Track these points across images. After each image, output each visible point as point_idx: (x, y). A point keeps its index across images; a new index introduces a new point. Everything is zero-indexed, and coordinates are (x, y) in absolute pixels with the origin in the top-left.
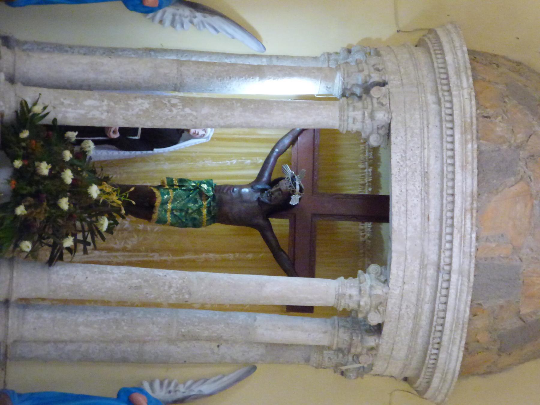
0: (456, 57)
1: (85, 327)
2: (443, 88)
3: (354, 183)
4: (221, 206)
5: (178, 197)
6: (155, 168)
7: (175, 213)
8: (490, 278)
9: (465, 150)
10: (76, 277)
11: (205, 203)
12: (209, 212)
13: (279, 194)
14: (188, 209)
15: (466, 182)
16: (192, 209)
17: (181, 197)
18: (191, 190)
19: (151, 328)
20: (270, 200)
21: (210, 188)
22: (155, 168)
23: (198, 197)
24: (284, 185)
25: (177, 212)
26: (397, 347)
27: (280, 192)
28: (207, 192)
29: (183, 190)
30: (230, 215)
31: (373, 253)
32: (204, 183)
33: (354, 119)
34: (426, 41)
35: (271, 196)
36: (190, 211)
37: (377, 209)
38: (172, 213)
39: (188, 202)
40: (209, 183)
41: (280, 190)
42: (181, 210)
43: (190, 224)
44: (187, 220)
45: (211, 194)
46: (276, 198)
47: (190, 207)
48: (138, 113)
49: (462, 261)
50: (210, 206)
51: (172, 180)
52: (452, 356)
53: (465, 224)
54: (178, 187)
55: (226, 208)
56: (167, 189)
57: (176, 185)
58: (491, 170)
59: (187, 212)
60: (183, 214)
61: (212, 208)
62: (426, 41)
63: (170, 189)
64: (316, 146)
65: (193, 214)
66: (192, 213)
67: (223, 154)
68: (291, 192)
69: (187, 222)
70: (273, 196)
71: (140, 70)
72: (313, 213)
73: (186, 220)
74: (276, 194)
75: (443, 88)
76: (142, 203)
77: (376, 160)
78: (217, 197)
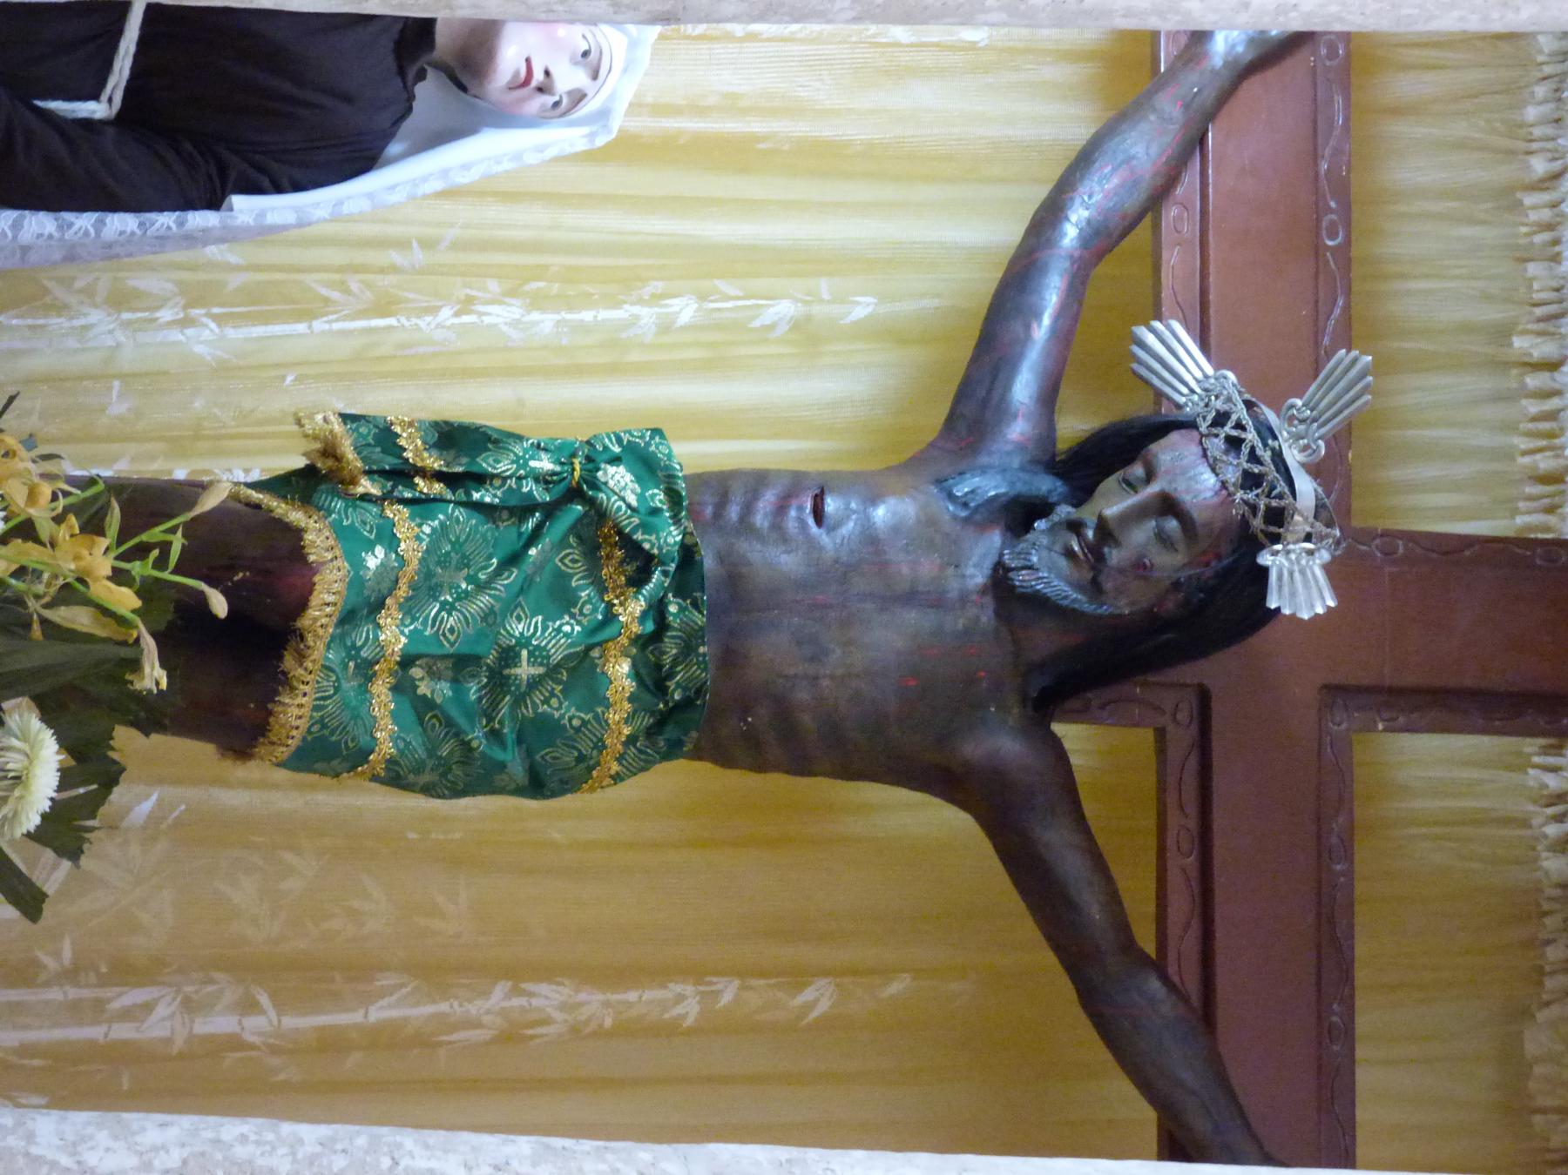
5: (443, 562)
7: (423, 689)
11: (633, 610)
12: (652, 679)
13: (1162, 538)
14: (509, 656)
16: (538, 655)
17: (465, 562)
18: (525, 508)
20: (1094, 588)
21: (658, 497)
23: (572, 562)
24: (1195, 475)
25: (433, 674)
27: (1172, 524)
28: (645, 527)
29: (479, 507)
30: (802, 695)
32: (615, 460)
35: (1096, 555)
36: (525, 670)
38: (402, 687)
39: (511, 606)
40: (647, 465)
41: (1168, 505)
42: (462, 664)
43: (514, 761)
44: (490, 738)
45: (673, 536)
46: (1140, 567)
47: (524, 642)
50: (662, 625)
51: (386, 436)
54: (438, 488)
55: (774, 650)
56: (366, 498)
57: (422, 472)
59: (499, 682)
60: (473, 691)
61: (671, 649)
63: (387, 497)
65: (538, 697)
66: (534, 683)
68: (1257, 523)
69: (498, 754)
70: (1115, 556)
73: (495, 735)
74: (1141, 535)
78: (708, 561)
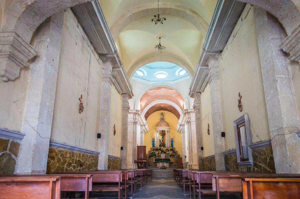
0: (156, 128)
1: (168, 143)
2: (158, 128)
3: (162, 132)
4: (163, 137)
6: (161, 141)
8: (165, 126)
9: (160, 127)
10: (166, 144)
15: (161, 127)
19: (168, 140)
22: (161, 141)
26: (168, 130)
31: (165, 131)
33: (159, 132)
34: (155, 129)
37: (163, 131)
48: (159, 141)
49: (164, 127)
52: (169, 127)
53: (163, 127)
58: (161, 126)
62: (155, 129)
64: (160, 133)
67: (161, 137)
71: (157, 141)
72: (163, 134)
75: (158, 128)
76: (163, 141)
77: (160, 131)
